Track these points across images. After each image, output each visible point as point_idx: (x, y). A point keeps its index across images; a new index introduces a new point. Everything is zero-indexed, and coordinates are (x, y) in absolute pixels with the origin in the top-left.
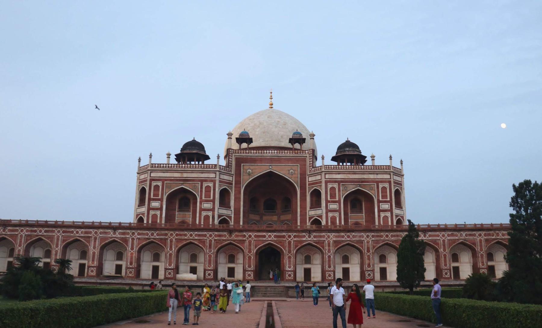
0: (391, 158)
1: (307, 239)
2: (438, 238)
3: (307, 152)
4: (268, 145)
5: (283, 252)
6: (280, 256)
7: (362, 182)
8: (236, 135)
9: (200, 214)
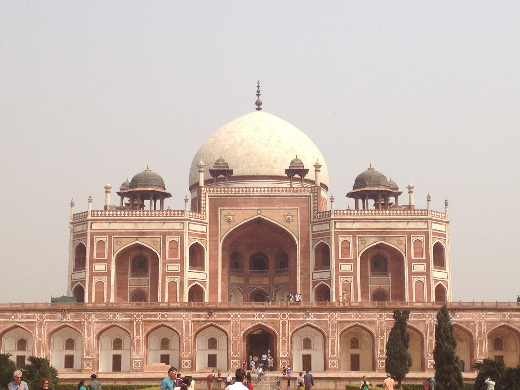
0: (429, 198)
2: (473, 320)
4: (255, 174)
5: (276, 335)
7: (387, 233)
9: (164, 280)
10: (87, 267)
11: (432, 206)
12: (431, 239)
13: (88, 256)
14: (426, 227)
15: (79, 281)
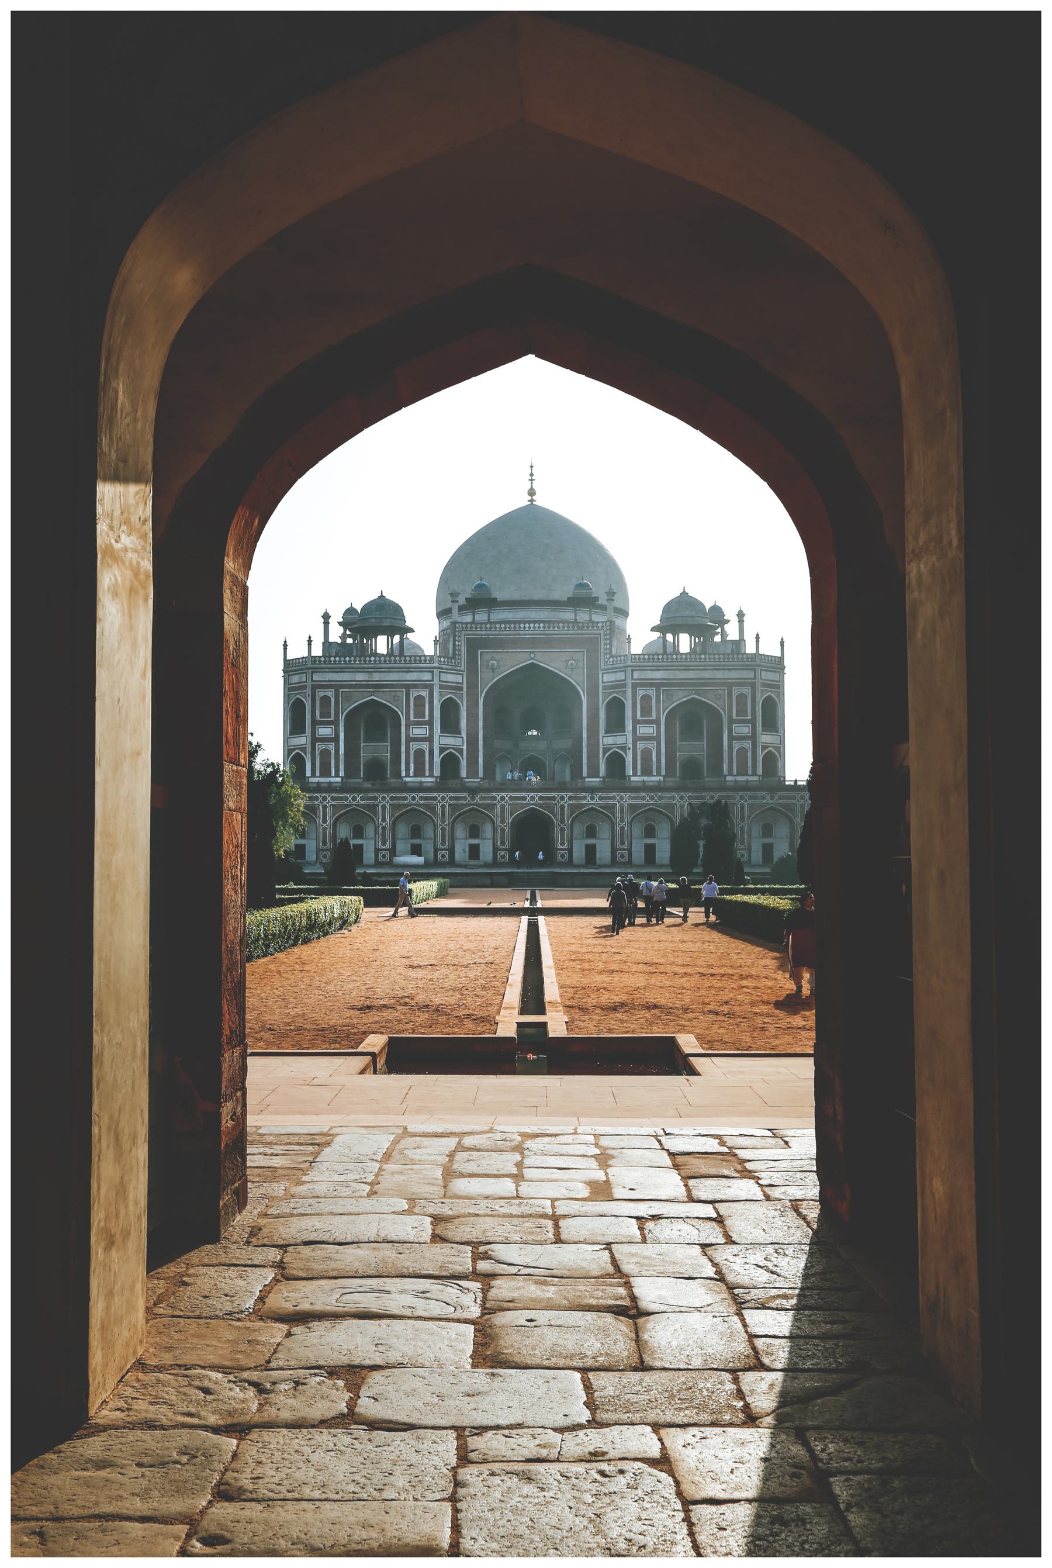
0: (757, 638)
1: (589, 801)
3: (600, 625)
4: (527, 599)
8: (466, 592)
12: (759, 694)
13: (308, 716)
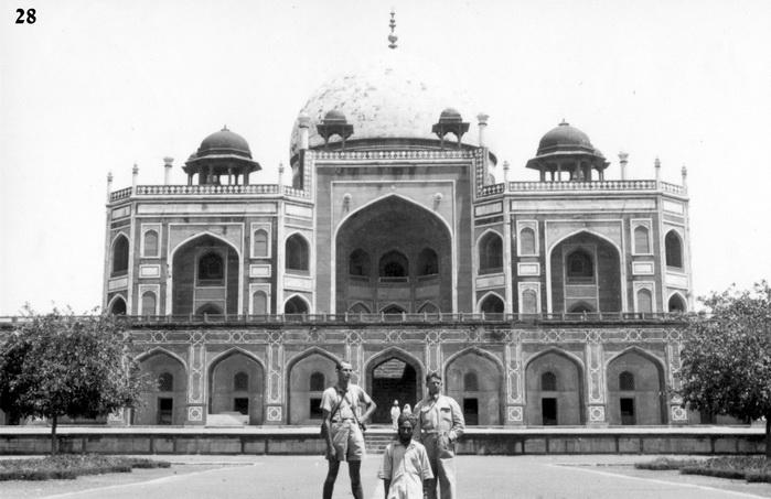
4: (387, 136)
5: (420, 368)
6: (415, 373)
9: (246, 290)
10: (131, 269)
11: (664, 175)
14: (654, 206)
15: (121, 292)
